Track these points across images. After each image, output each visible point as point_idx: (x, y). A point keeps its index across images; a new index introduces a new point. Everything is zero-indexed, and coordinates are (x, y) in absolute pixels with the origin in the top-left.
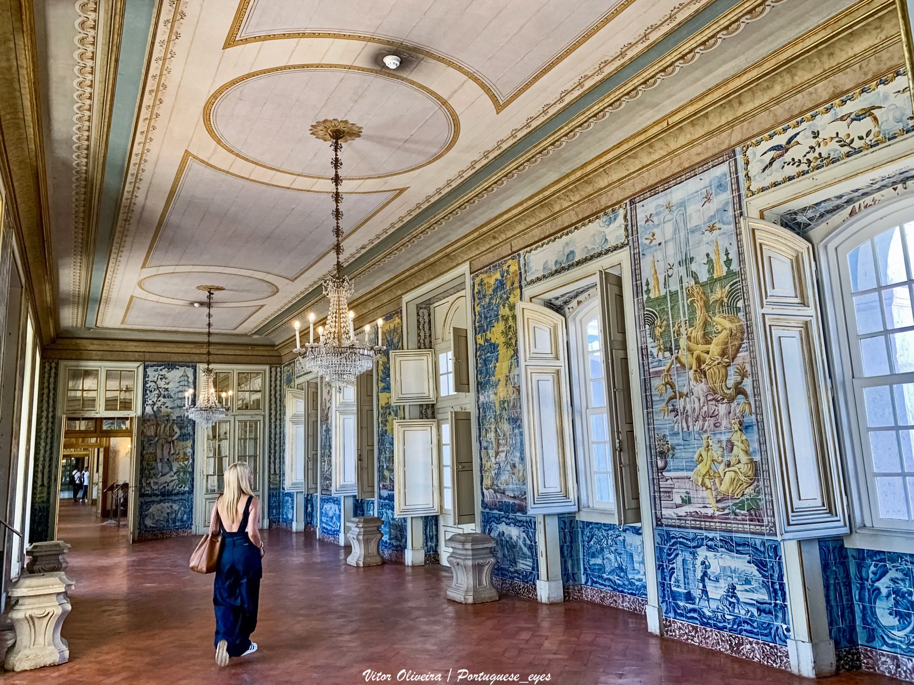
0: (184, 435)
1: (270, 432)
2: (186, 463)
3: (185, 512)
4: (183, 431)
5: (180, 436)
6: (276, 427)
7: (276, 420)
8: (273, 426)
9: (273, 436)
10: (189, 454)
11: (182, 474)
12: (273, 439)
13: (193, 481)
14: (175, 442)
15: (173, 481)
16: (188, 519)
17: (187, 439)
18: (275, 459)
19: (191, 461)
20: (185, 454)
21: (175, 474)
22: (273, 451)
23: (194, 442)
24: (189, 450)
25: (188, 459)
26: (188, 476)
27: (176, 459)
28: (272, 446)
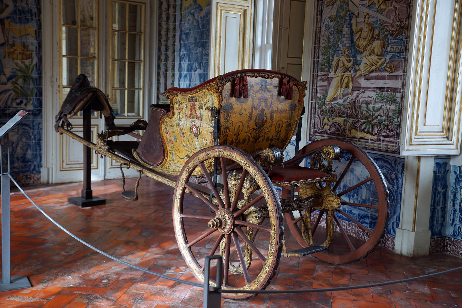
0: (22, 12)
1: (160, 25)
2: (27, 62)
3: (29, 145)
4: (19, 4)
5: (14, 12)
6: (168, 18)
7: (169, 6)
8: (164, 16)
9: (163, 33)
10: (33, 48)
11: (20, 81)
12: (164, 38)
13: (41, 94)
14: (7, 22)
15: (5, 91)
16: (35, 157)
17: (27, 21)
18: (166, 70)
19: (35, 60)
20: (25, 46)
21: (9, 79)
22: (163, 57)
23: (40, 27)
24: (32, 41)
25: (30, 57)
26: (32, 86)
27: (10, 54)
28: (163, 48)
